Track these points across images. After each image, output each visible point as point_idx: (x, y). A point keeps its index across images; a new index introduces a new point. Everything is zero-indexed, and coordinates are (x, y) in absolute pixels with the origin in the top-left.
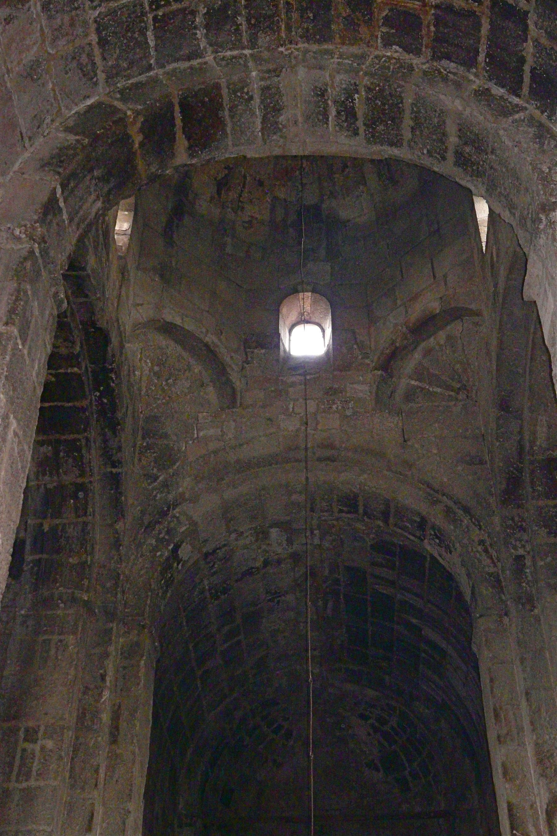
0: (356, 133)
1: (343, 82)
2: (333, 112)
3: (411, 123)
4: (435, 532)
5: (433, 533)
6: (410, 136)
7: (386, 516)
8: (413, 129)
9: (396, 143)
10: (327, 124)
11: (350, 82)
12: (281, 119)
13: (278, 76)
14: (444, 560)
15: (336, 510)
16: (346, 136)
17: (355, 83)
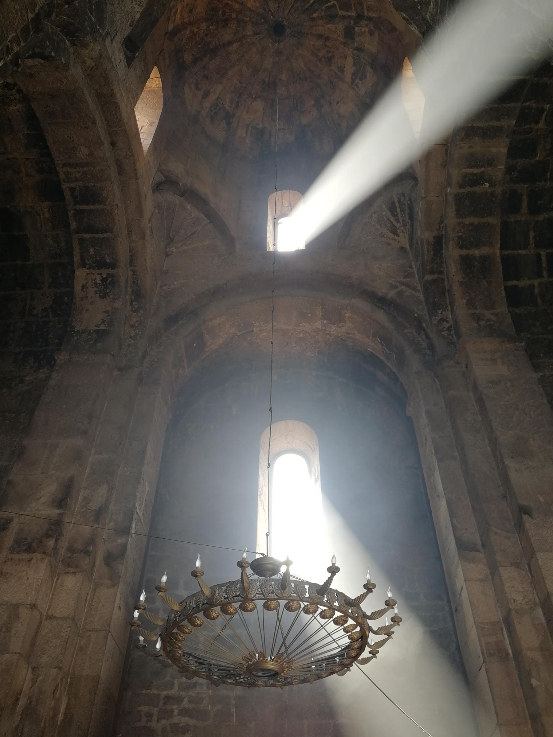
0: (461, 186)
1: (497, 177)
2: (476, 171)
3: (476, 223)
4: (106, 278)
5: (104, 276)
6: (467, 223)
7: (90, 229)
8: (472, 224)
9: (459, 213)
10: (468, 168)
11: (497, 181)
12: (477, 138)
13: (507, 137)
14: (82, 290)
15: (73, 185)
16: (459, 180)
17: (496, 185)
